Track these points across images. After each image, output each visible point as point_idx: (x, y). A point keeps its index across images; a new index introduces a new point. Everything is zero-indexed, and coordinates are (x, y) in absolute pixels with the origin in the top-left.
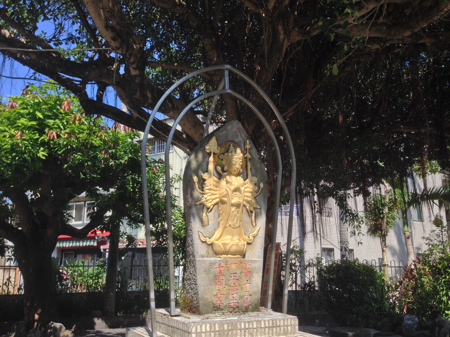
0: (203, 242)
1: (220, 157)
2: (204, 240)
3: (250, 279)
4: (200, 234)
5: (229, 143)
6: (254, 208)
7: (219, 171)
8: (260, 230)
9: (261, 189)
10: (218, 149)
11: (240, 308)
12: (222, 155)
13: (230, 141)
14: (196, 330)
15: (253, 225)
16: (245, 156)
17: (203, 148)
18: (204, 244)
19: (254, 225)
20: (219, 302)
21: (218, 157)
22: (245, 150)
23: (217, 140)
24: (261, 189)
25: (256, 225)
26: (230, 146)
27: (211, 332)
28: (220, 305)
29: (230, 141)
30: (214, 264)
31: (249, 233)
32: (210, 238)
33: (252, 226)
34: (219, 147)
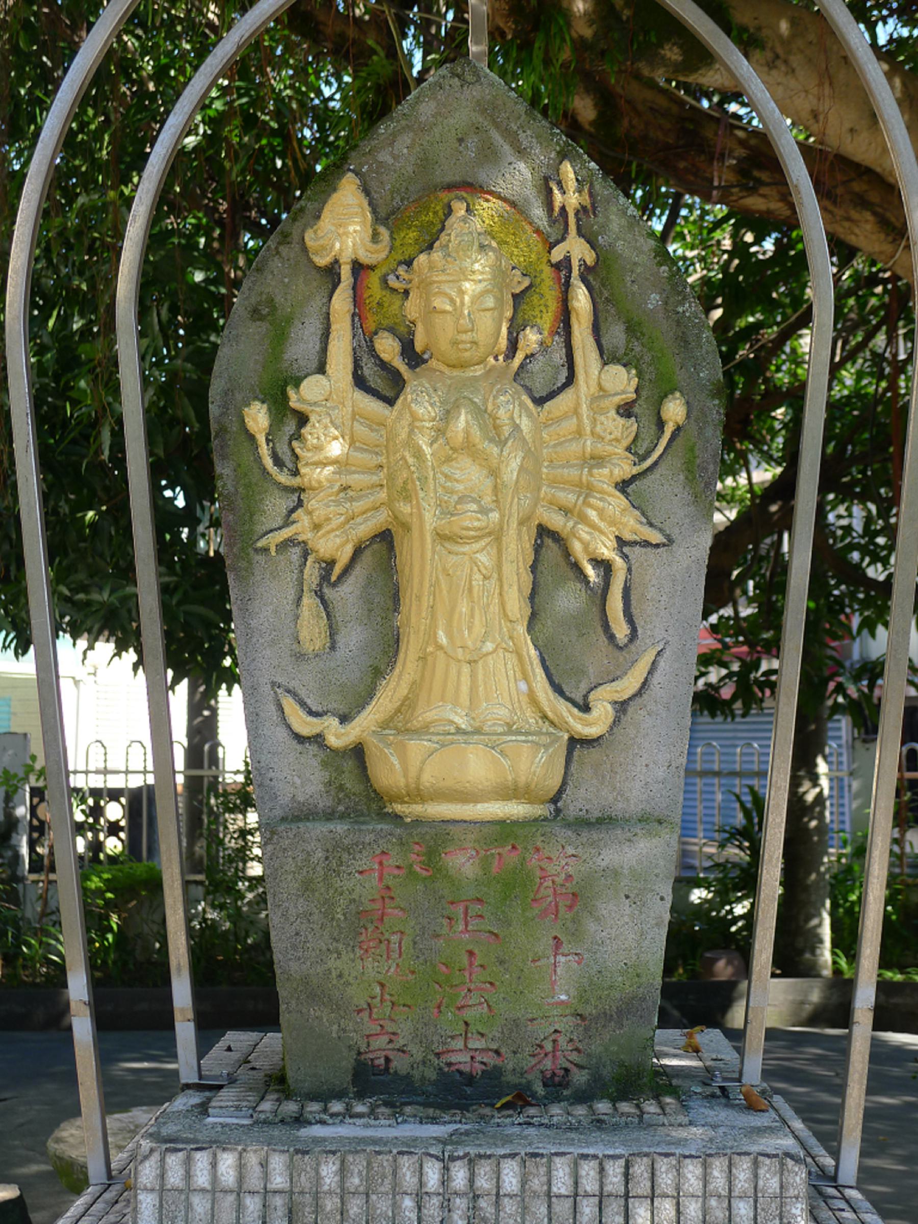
0: (300, 739)
1: (392, 282)
2: (305, 731)
3: (576, 934)
4: (289, 703)
5: (445, 196)
6: (621, 542)
7: (385, 356)
8: (662, 664)
9: (669, 430)
10: (375, 237)
11: (580, 1078)
12: (401, 270)
13: (450, 187)
14: (162, 1176)
15: (611, 637)
16: (557, 254)
17: (297, 248)
18: (313, 749)
19: (621, 631)
20: (381, 1042)
21: (384, 281)
22: (552, 222)
23: (367, 192)
24: (669, 430)
25: (633, 635)
26: (449, 211)
27: (240, 1191)
28: (388, 1060)
29: (450, 187)
30: (347, 850)
31: (584, 687)
32: (344, 719)
33: (603, 639)
34: (383, 230)
